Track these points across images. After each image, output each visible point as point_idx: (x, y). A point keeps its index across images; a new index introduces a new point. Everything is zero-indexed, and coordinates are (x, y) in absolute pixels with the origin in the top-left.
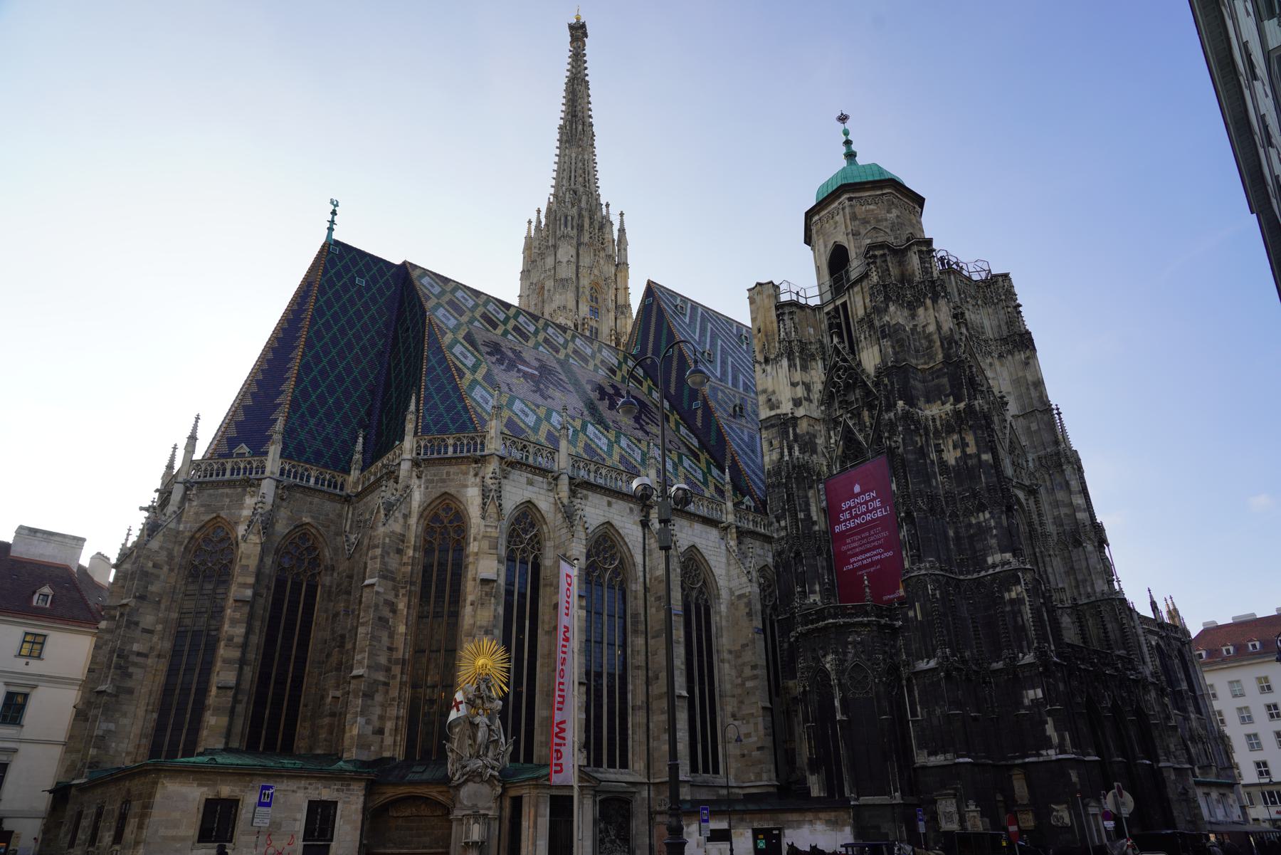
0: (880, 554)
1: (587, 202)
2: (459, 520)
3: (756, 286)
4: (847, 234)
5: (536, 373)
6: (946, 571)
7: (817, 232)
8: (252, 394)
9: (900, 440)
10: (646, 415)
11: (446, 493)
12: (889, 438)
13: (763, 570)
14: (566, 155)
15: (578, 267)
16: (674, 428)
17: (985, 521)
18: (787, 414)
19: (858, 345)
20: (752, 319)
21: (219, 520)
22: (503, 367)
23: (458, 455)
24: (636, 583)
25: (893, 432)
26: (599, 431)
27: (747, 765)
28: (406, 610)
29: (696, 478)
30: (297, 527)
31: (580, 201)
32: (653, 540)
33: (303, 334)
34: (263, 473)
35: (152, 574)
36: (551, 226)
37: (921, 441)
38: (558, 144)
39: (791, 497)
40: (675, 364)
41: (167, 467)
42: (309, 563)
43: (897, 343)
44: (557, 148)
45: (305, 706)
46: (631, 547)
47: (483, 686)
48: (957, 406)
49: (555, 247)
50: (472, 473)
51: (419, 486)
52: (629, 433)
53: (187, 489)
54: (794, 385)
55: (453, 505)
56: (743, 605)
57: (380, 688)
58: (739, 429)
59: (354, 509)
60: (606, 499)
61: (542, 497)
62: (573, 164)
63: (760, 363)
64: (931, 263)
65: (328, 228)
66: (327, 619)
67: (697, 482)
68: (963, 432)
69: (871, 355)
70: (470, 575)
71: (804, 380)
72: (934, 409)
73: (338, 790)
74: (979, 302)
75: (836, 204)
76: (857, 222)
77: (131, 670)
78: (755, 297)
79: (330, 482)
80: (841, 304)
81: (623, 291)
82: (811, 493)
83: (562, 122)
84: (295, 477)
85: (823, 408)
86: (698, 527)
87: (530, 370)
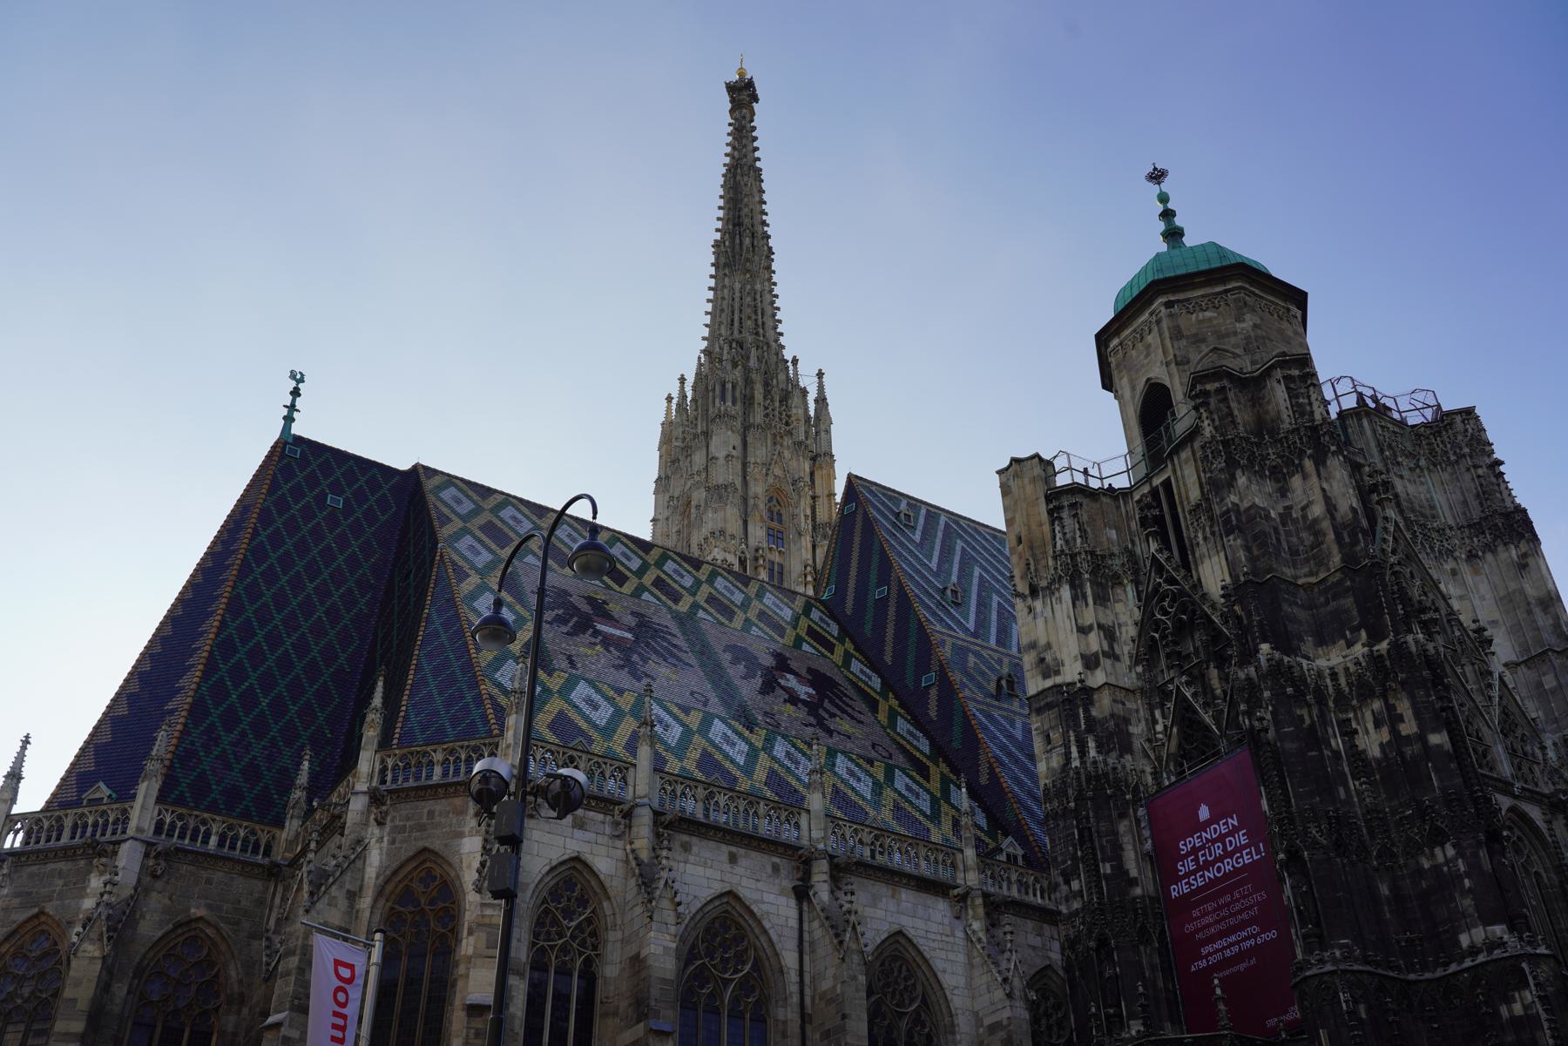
0: (1254, 936)
1: (759, 360)
2: (447, 894)
3: (1011, 464)
4: (1168, 364)
5: (629, 636)
6: (1378, 964)
7: (1118, 365)
9: (1269, 717)
10: (832, 702)
11: (425, 850)
12: (1249, 714)
13: (1039, 979)
15: (745, 465)
17: (1447, 862)
18: (1073, 684)
20: (1007, 521)
21: (43, 919)
22: (565, 629)
23: (451, 779)
24: (785, 1006)
25: (1255, 702)
30: (178, 926)
31: (748, 358)
32: (816, 924)
33: (226, 590)
34: (124, 832)
36: (700, 402)
37: (1311, 717)
38: (712, 271)
39: (1086, 834)
40: (892, 611)
44: (711, 276)
46: (774, 938)
48: (1375, 648)
49: (707, 434)
51: (381, 840)
54: (1083, 630)
55: (438, 872)
58: (1005, 718)
60: (725, 849)
61: (603, 850)
62: (737, 299)
63: (1022, 596)
64: (1309, 397)
65: (285, 418)
67: (917, 815)
69: (1217, 568)
70: (457, 1003)
71: (1103, 621)
72: (1333, 655)
74: (1423, 463)
75: (1145, 316)
76: (1184, 342)
78: (1011, 483)
79: (245, 840)
80: (1162, 483)
81: (826, 499)
82: (1123, 827)
83: (718, 236)
84: (182, 836)
85: (1139, 669)
86: (907, 897)
87: (618, 632)
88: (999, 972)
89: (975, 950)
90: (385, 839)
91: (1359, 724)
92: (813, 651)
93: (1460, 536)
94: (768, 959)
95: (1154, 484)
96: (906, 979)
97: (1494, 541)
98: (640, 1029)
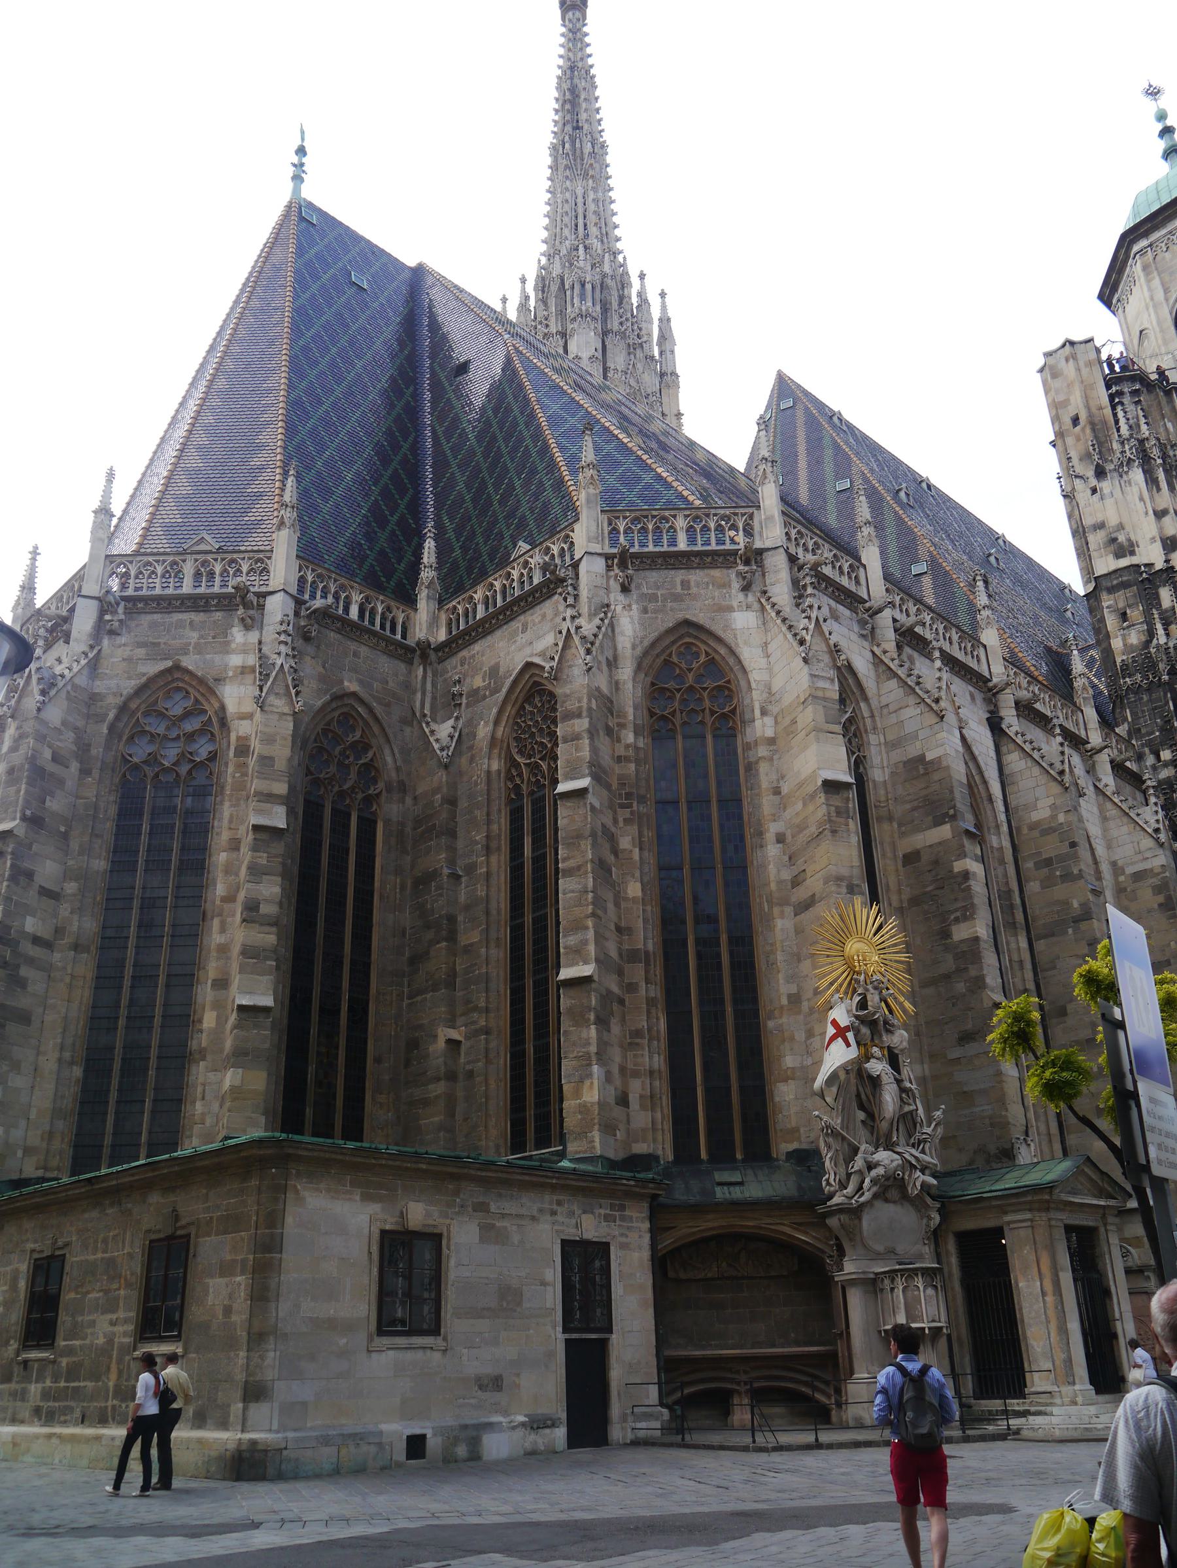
3: (1064, 346)
8: (199, 448)
11: (687, 623)
14: (567, 189)
24: (999, 834)
28: (637, 850)
30: (336, 698)
35: (52, 775)
41: (23, 587)
42: (359, 773)
45: (378, 1060)
47: (873, 999)
49: (564, 335)
50: (736, 585)
53: (102, 612)
54: (1160, 514)
55: (703, 647)
56: (1149, 892)
57: (615, 1006)
59: (435, 674)
62: (580, 204)
66: (403, 888)
73: (607, 1218)
77: (24, 971)
88: (1146, 823)
89: (1109, 805)
90: (634, 607)
98: (945, 831)
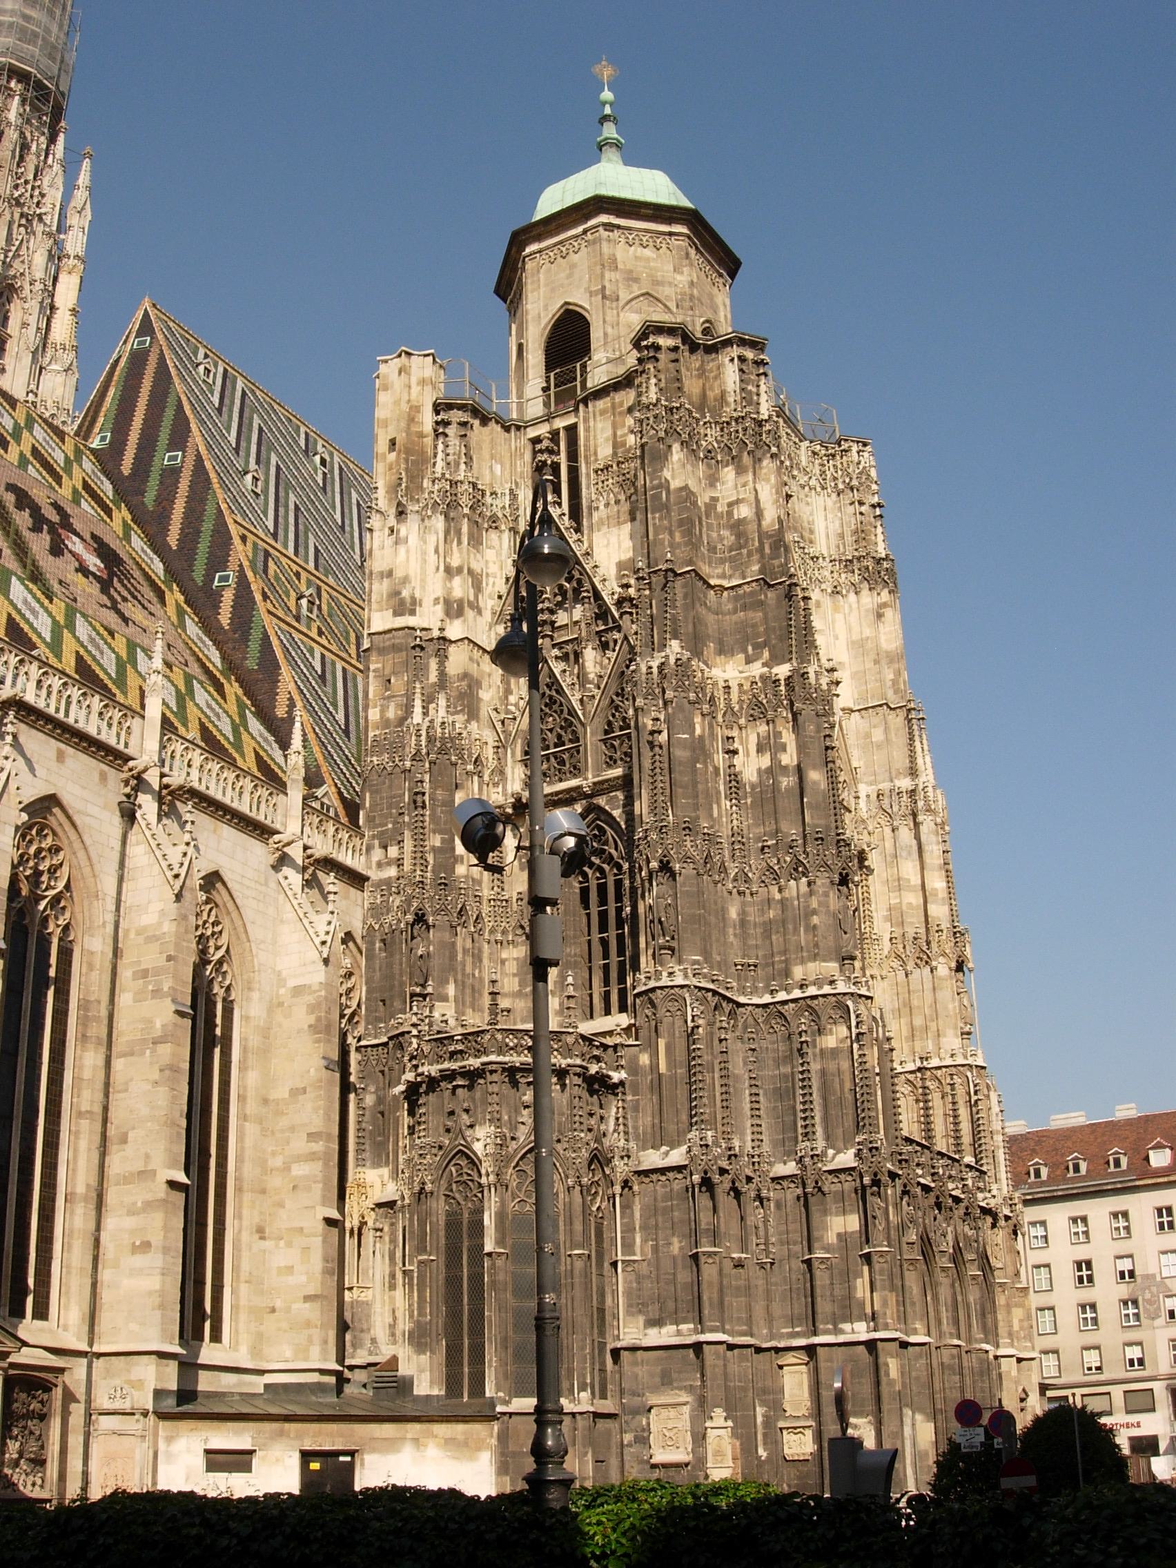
4: (591, 294)
10: (121, 581)
16: (174, 618)
19: (590, 515)
26: (34, 596)
27: (279, 1329)
29: (220, 731)
43: (680, 526)
48: (775, 670)
52: (90, 612)
56: (304, 1009)
64: (758, 386)
67: (223, 741)
68: (779, 721)
69: (614, 540)
74: (813, 482)
75: (580, 229)
86: (229, 834)
91: (742, 743)
92: (92, 512)
93: (830, 568)
94: (83, 878)
95: (555, 427)
96: (214, 924)
97: (861, 582)
